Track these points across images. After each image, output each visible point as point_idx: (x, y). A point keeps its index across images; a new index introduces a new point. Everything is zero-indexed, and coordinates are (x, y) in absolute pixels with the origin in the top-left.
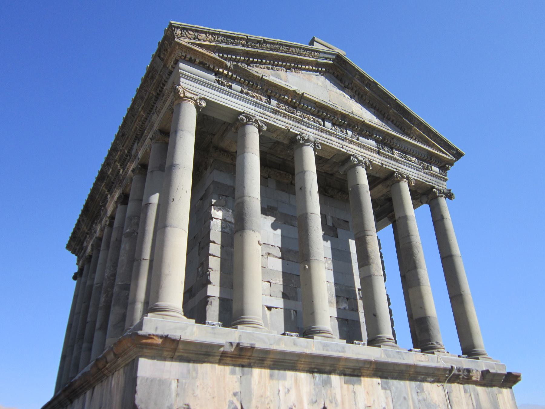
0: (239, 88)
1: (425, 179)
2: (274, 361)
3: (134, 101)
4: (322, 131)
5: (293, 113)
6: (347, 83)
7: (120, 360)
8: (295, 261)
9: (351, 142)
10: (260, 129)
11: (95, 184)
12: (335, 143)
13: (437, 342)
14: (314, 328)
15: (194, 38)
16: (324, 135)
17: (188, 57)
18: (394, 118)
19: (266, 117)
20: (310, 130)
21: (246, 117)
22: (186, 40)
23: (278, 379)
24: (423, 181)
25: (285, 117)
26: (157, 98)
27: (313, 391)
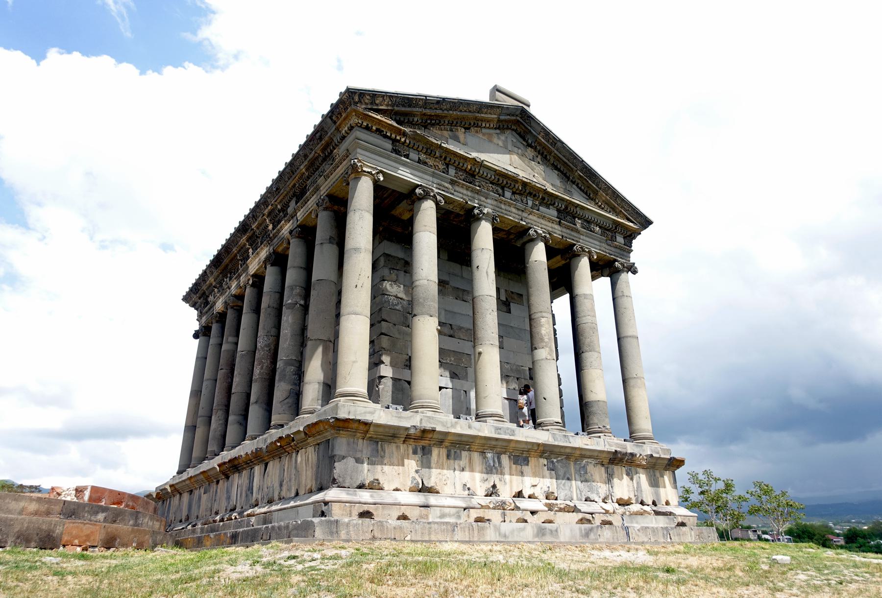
3: (296, 157)
5: (470, 183)
6: (530, 141)
7: (310, 440)
10: (437, 204)
11: (232, 235)
15: (372, 103)
16: (503, 206)
20: (489, 201)
21: (424, 191)
23: (455, 459)
26: (324, 160)
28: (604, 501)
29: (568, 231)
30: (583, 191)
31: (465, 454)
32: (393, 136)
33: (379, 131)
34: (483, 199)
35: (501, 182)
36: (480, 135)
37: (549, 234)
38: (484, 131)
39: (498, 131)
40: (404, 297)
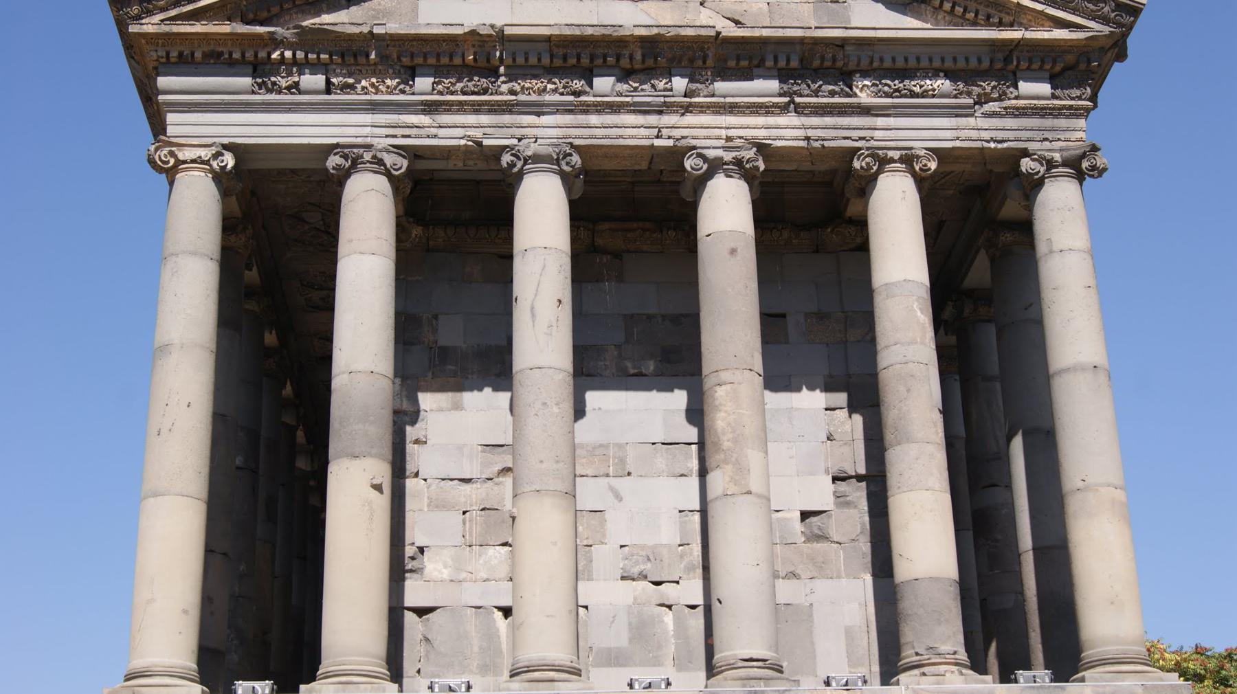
0: (319, 80)
1: (986, 135)
4: (586, 109)
5: (485, 91)
8: (589, 472)
9: (687, 109)
10: (388, 174)
12: (633, 131)
16: (594, 119)
17: (174, 54)
19: (407, 132)
20: (546, 120)
21: (345, 157)
22: (157, 18)
24: (978, 144)
25: (465, 112)
29: (828, 120)
32: (249, 55)
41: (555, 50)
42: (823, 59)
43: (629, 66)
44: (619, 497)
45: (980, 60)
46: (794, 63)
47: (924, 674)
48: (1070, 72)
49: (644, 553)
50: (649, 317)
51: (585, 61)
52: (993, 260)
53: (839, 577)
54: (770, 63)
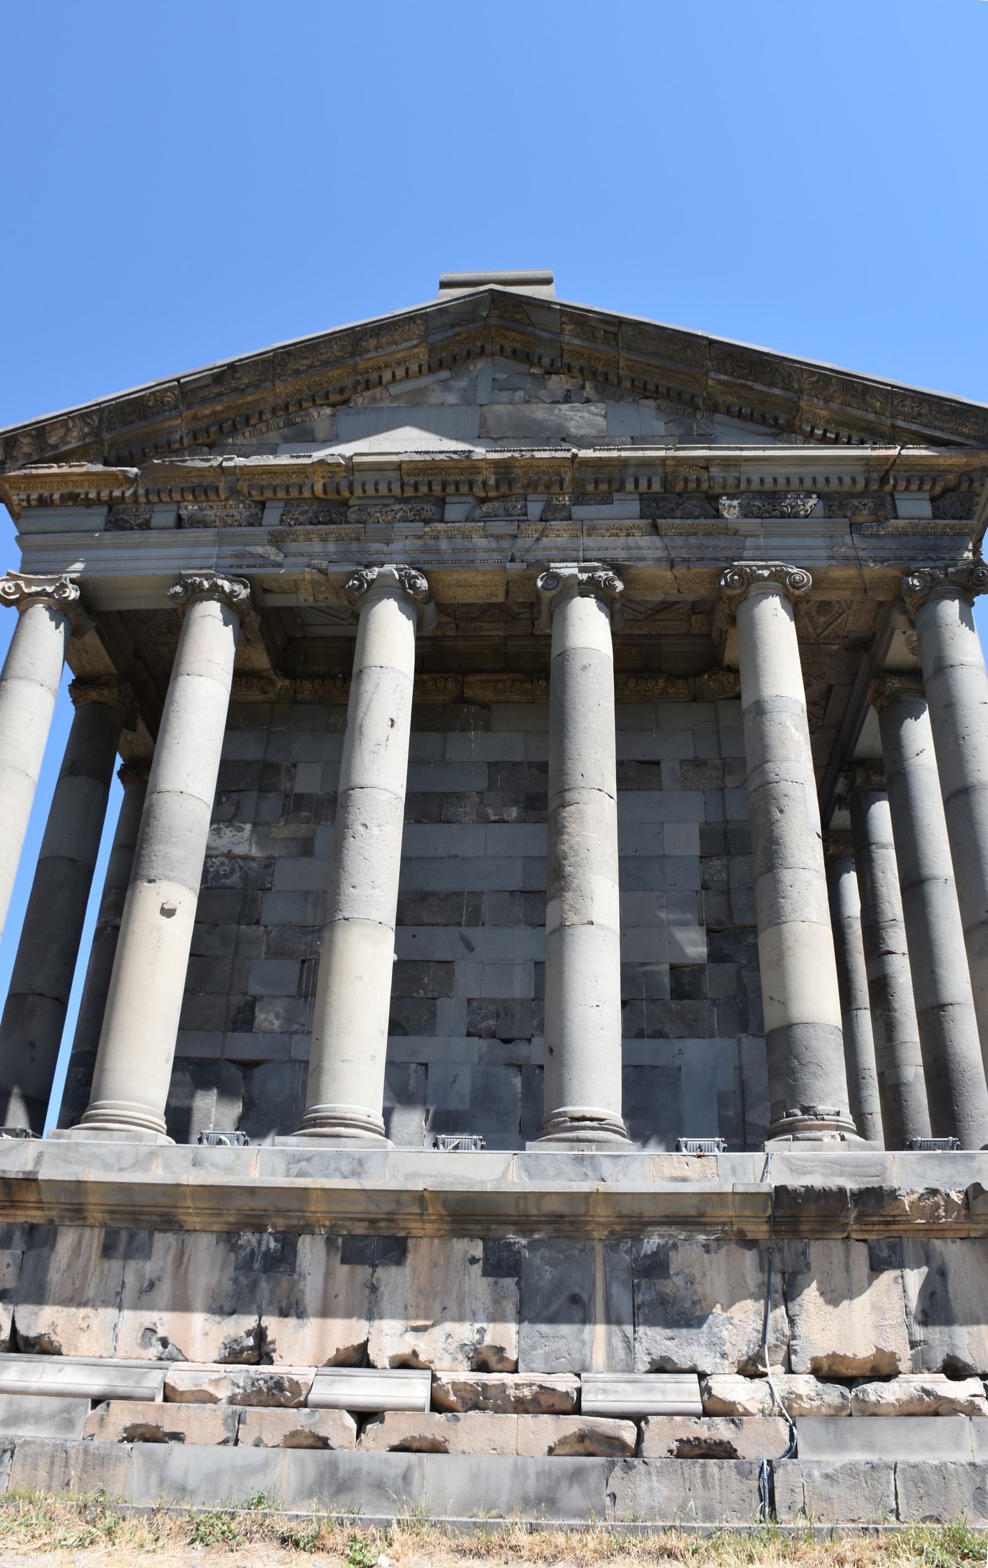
2: (112, 1212)
6: (546, 361)
9: (543, 534)
10: (227, 601)
13: (806, 1110)
14: (316, 1111)
17: (34, 496)
18: (730, 399)
21: (185, 586)
23: (127, 1257)
27: (228, 1286)
28: (751, 1369)
29: (692, 540)
30: (751, 418)
31: (164, 1242)
32: (104, 495)
33: (72, 498)
34: (377, 546)
35: (424, 489)
36: (387, 403)
37: (619, 570)
38: (394, 390)
39: (445, 374)
40: (255, 851)
41: (406, 479)
42: (686, 481)
43: (483, 494)
44: (470, 947)
45: (854, 481)
46: (656, 487)
47: (795, 1139)
48: (952, 494)
49: (492, 1008)
50: (515, 765)
51: (437, 489)
52: (880, 712)
53: (712, 1036)
54: (630, 486)
